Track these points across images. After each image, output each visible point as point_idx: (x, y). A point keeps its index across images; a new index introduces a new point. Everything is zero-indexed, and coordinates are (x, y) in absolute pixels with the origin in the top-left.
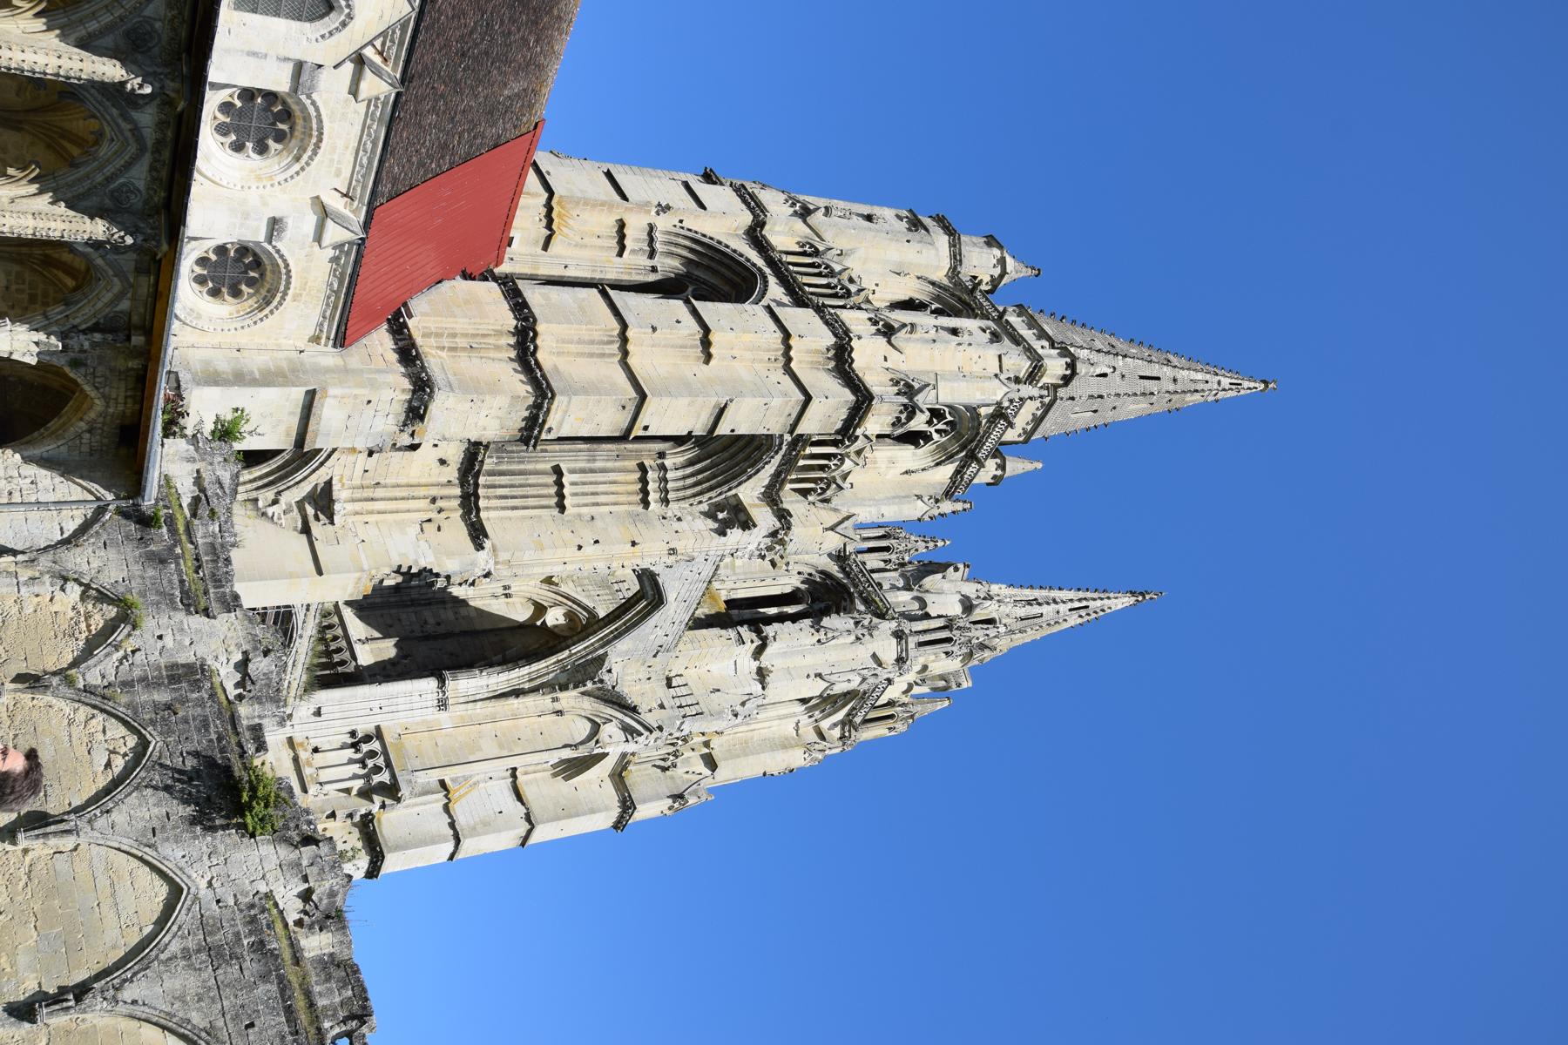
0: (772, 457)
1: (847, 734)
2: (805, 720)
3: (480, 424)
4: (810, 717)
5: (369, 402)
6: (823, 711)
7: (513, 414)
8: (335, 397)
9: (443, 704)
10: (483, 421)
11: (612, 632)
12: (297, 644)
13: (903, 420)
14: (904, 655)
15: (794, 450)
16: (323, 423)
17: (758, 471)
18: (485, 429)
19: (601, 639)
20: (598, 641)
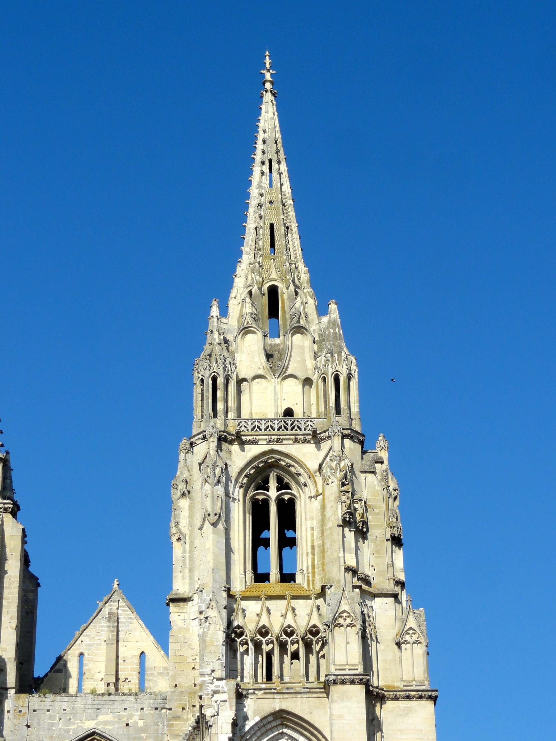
1: (327, 434)
2: (310, 490)
4: (305, 485)
6: (299, 475)
14: (201, 436)
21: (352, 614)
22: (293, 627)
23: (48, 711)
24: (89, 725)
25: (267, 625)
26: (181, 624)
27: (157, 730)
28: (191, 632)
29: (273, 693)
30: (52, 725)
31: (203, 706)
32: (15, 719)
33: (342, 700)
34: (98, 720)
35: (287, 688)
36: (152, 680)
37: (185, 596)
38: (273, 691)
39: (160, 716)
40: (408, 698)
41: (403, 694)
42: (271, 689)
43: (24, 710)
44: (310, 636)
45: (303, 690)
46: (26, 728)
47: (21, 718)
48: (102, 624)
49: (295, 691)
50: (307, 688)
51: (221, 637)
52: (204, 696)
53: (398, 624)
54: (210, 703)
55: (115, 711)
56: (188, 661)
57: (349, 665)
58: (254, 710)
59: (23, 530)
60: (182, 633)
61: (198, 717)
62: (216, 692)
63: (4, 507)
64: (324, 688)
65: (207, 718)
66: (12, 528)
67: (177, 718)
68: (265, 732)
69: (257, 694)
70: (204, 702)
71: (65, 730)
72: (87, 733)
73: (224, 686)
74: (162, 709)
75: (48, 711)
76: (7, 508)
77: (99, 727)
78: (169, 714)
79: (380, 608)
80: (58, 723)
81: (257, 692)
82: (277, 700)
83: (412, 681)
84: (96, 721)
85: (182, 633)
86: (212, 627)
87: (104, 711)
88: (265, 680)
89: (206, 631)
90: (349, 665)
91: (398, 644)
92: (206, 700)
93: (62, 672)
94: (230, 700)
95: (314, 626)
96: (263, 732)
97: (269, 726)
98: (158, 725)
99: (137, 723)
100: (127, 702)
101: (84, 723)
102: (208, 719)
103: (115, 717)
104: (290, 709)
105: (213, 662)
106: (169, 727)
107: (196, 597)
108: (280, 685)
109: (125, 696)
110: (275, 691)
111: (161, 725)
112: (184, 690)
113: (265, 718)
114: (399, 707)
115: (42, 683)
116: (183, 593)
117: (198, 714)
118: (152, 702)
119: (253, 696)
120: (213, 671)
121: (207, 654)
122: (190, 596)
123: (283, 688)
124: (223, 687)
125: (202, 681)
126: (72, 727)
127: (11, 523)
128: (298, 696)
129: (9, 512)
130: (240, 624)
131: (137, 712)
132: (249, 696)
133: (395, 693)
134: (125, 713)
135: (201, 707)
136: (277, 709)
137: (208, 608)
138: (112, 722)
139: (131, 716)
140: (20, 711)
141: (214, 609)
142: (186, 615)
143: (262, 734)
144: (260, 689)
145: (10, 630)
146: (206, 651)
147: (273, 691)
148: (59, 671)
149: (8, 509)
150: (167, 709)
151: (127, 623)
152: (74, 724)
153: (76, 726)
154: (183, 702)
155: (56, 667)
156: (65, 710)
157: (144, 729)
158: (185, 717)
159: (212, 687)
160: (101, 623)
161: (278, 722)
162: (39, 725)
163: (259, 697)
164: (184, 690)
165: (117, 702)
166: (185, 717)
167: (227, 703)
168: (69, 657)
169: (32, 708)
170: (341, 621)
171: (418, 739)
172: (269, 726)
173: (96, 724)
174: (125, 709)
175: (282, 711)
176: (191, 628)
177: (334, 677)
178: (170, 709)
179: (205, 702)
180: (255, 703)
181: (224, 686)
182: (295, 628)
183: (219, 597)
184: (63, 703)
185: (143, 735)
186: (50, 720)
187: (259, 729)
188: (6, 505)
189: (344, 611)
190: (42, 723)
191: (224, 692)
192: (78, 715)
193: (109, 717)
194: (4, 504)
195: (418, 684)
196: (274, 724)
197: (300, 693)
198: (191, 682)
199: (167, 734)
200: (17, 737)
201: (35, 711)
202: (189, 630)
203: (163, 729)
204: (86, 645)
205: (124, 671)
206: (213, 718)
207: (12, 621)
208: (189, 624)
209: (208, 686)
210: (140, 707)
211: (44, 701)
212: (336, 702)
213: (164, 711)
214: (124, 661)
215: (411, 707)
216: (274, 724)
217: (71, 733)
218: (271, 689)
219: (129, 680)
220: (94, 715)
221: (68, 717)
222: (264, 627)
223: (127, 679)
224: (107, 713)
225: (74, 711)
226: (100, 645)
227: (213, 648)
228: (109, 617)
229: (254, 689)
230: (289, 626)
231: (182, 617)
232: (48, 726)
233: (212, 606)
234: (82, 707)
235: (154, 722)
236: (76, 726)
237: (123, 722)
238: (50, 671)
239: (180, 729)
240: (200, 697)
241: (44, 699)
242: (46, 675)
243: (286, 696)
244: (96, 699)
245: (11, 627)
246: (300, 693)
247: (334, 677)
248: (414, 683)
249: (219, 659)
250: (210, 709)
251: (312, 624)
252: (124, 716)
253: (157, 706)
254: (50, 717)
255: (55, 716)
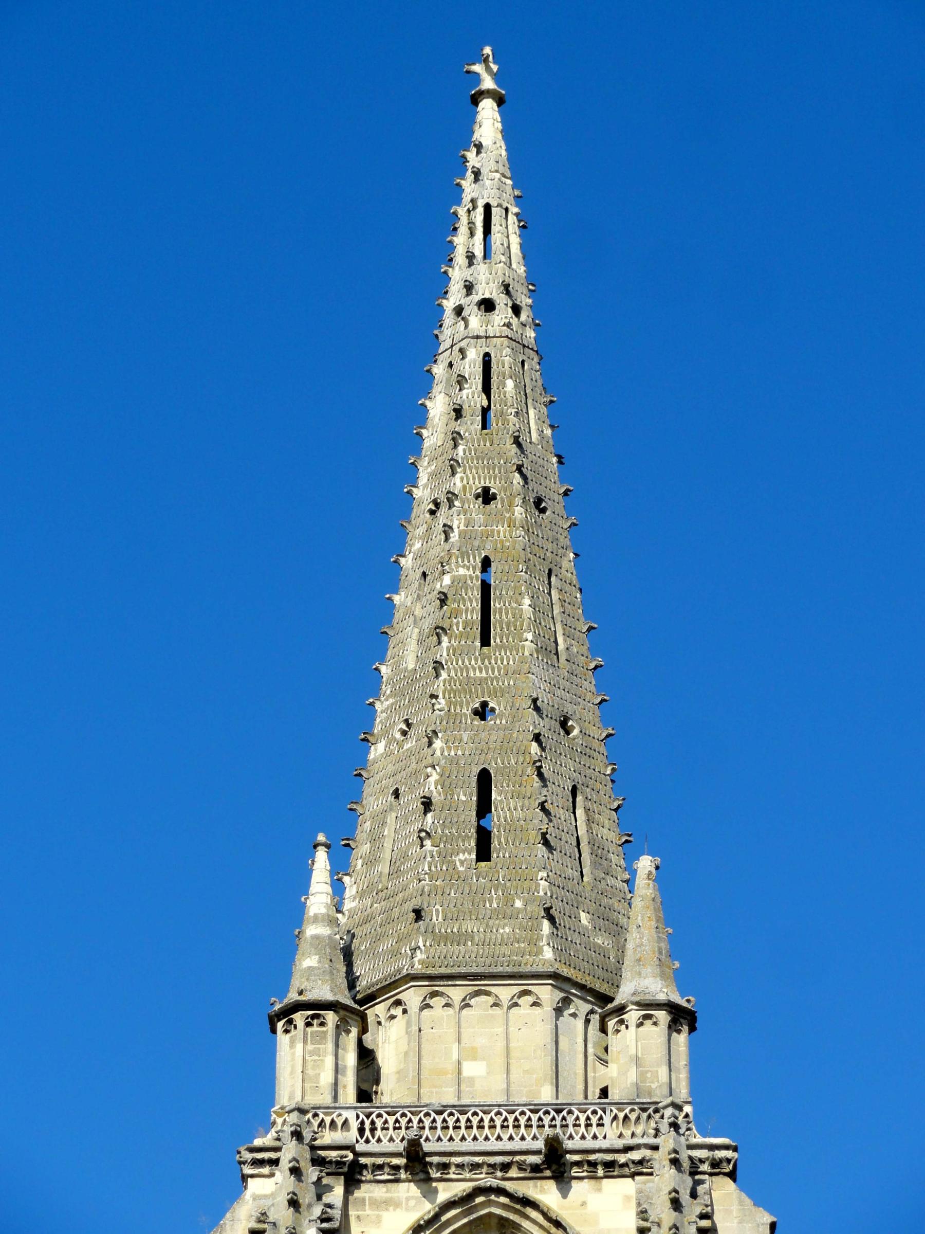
59: (773, 1226)
63: (714, 1159)
66: (740, 1222)
76: (721, 1161)
127: (735, 1208)
129: (725, 1174)
149: (725, 1164)
188: (717, 1152)
194: (712, 1147)
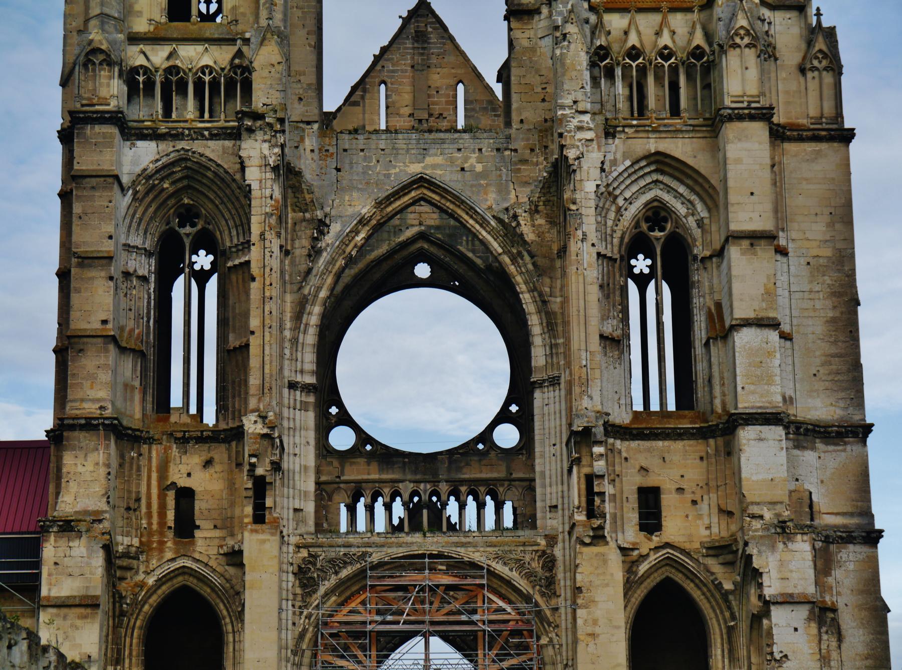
0: (194, 152)
3: (91, 468)
5: (56, 564)
7: (82, 445)
8: (50, 590)
9: (554, 382)
10: (90, 467)
11: (471, 217)
12: (433, 548)
13: (101, 57)
15: (183, 134)
16: (75, 594)
17: (210, 160)
18: (97, 464)
19: (481, 225)
20: (484, 229)
21: (752, 32)
22: (671, 49)
23: (362, 150)
24: (415, 169)
25: (638, 45)
26: (525, 43)
27: (500, 176)
28: (538, 54)
29: (648, 131)
30: (369, 167)
31: (565, 146)
32: (320, 160)
33: (740, 140)
34: (426, 163)
35: (665, 125)
36: (473, 116)
37: (531, 7)
38: (647, 128)
39: (503, 158)
40: (816, 139)
41: (809, 133)
42: (645, 126)
43: (332, 150)
44: (693, 60)
45: (684, 128)
46: (335, 171)
47: (329, 159)
48: (408, 46)
49: (674, 129)
50: (690, 125)
51: (583, 59)
52: (566, 134)
53: (804, 46)
54: (573, 142)
55: (446, 151)
56: (535, 91)
57: (748, 96)
58: (624, 152)
60: (528, 55)
61: (556, 159)
62: (580, 128)
64: (712, 125)
65: (569, 160)
67: (524, 161)
68: (636, 180)
69: (627, 133)
70: (566, 141)
71: (385, 175)
72: (412, 179)
73: (590, 122)
74: (506, 149)
75: (362, 150)
77: (427, 172)
78: (515, 156)
79: (781, 25)
80: (375, 166)
81: (627, 130)
82: (652, 141)
83: (821, 118)
84: (422, 165)
85: (528, 55)
86: (572, 46)
87: (432, 151)
88: (636, 115)
89: (565, 51)
90: (748, 96)
91: (802, 70)
92: (568, 138)
93: (359, 105)
94: (597, 140)
95: (698, 47)
96: (633, 179)
97: (641, 173)
98: (501, 170)
99: (475, 167)
100: (460, 141)
101: (408, 166)
102: (571, 162)
103: (446, 160)
104: (668, 152)
105: (575, 91)
106: (515, 173)
107: (545, 10)
108: (655, 121)
109: (459, 134)
110: (650, 129)
111: (504, 170)
112: (532, 127)
113: (637, 161)
114: (805, 150)
115: (335, 118)
116: (528, 4)
117: (557, 157)
118: (492, 141)
119: (623, 136)
120: (575, 102)
121: (567, 81)
122: (536, 7)
123: (659, 126)
124: (587, 123)
125: (562, 114)
126: (393, 171)
128: (678, 136)
130: (603, 44)
131: (475, 153)
132: (618, 136)
133: (801, 133)
134: (459, 155)
135: (562, 147)
136: (653, 151)
137: (566, 22)
138: (442, 165)
139: (466, 159)
140: (327, 151)
141: (575, 24)
142: (532, 32)
143: (632, 182)
144: (632, 126)
145: (308, 48)
146: (566, 77)
147: (647, 128)
148: (356, 104)
150: (511, 150)
151: (440, 44)
152: (395, 167)
153: (397, 170)
154: (531, 142)
155: (352, 99)
156: (383, 150)
157: (483, 175)
158: (535, 160)
159: (575, 122)
160: (406, 44)
161: (653, 168)
162: (352, 168)
163: (630, 136)
164: (532, 127)
165: (447, 141)
166: (535, 160)
167: (595, 142)
168: (368, 86)
169: (341, 147)
170: (738, 40)
171: (830, 190)
172: (641, 173)
173: (423, 168)
174: (459, 150)
175: (658, 153)
176: (538, 49)
177: (730, 111)
178: (516, 151)
179: (567, 141)
180: (624, 143)
181: (590, 122)
182: (674, 49)
183: (580, 8)
184: (381, 142)
185: (482, 182)
186: (365, 162)
187: (630, 175)
189: (742, 27)
190: (355, 166)
191: (590, 129)
192: (400, 156)
193: (439, 160)
195: (829, 121)
196: (647, 170)
197: (682, 131)
198: (541, 116)
199: (513, 181)
200: (324, 182)
201: (345, 150)
202: (536, 51)
203: (507, 175)
204: (389, 71)
205: (437, 104)
206: (577, 161)
207: (310, 37)
208: (536, 44)
209: (570, 121)
210: (477, 147)
211: (357, 139)
212: (732, 142)
213: (507, 153)
214: (437, 92)
215: (820, 151)
216: (647, 170)
217: (392, 179)
218: (645, 126)
219: (444, 116)
220: (420, 157)
221: (388, 159)
222: (634, 47)
223: (441, 114)
224: (436, 155)
225: (395, 152)
226: (406, 72)
227: (574, 73)
228: (417, 36)
229: (624, 126)
230: (666, 47)
231: (526, 35)
232: (363, 169)
233: (572, 19)
234: (405, 146)
235: (496, 166)
236: (397, 170)
237: (457, 166)
238: (344, 104)
239: (529, 175)
240: (561, 135)
241: (356, 136)
242: (339, 109)
243: (663, 135)
244: (422, 137)
245: (310, 45)
246: (682, 131)
247: (730, 111)
248: (824, 120)
249: (583, 87)
250: (574, 150)
251: (695, 45)
252: (458, 158)
253: (498, 146)
254: (365, 158)
255: (370, 158)
